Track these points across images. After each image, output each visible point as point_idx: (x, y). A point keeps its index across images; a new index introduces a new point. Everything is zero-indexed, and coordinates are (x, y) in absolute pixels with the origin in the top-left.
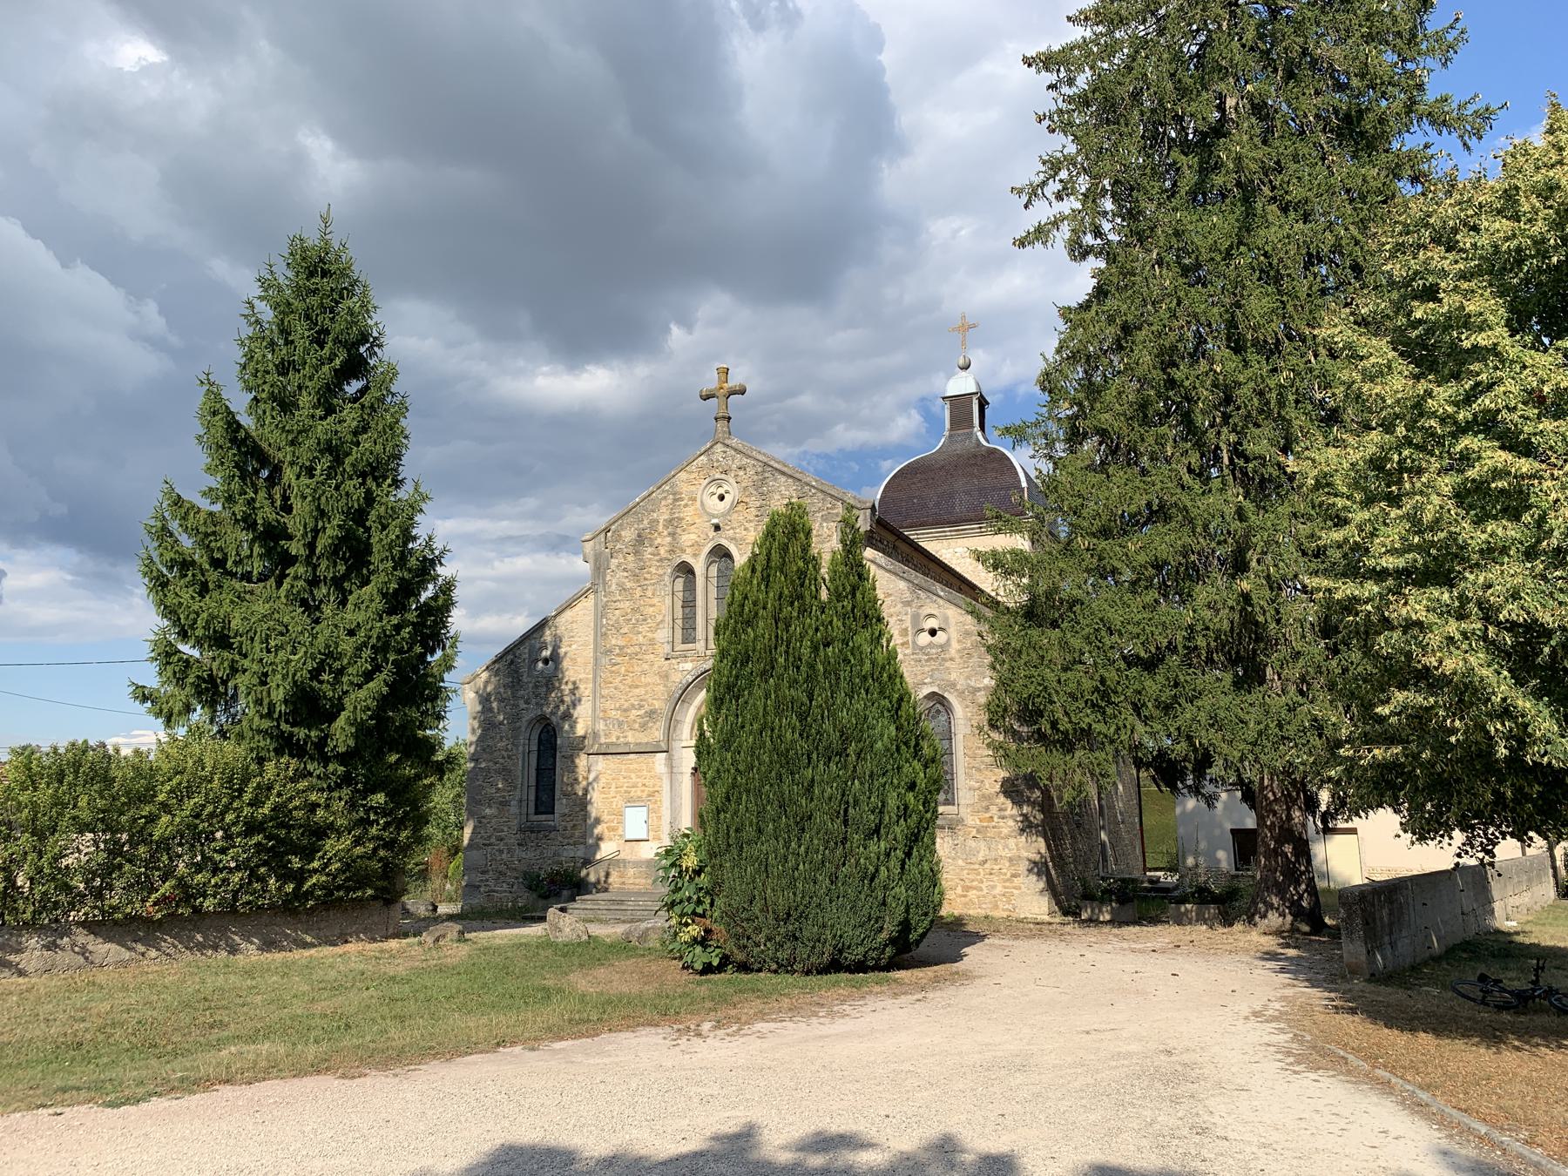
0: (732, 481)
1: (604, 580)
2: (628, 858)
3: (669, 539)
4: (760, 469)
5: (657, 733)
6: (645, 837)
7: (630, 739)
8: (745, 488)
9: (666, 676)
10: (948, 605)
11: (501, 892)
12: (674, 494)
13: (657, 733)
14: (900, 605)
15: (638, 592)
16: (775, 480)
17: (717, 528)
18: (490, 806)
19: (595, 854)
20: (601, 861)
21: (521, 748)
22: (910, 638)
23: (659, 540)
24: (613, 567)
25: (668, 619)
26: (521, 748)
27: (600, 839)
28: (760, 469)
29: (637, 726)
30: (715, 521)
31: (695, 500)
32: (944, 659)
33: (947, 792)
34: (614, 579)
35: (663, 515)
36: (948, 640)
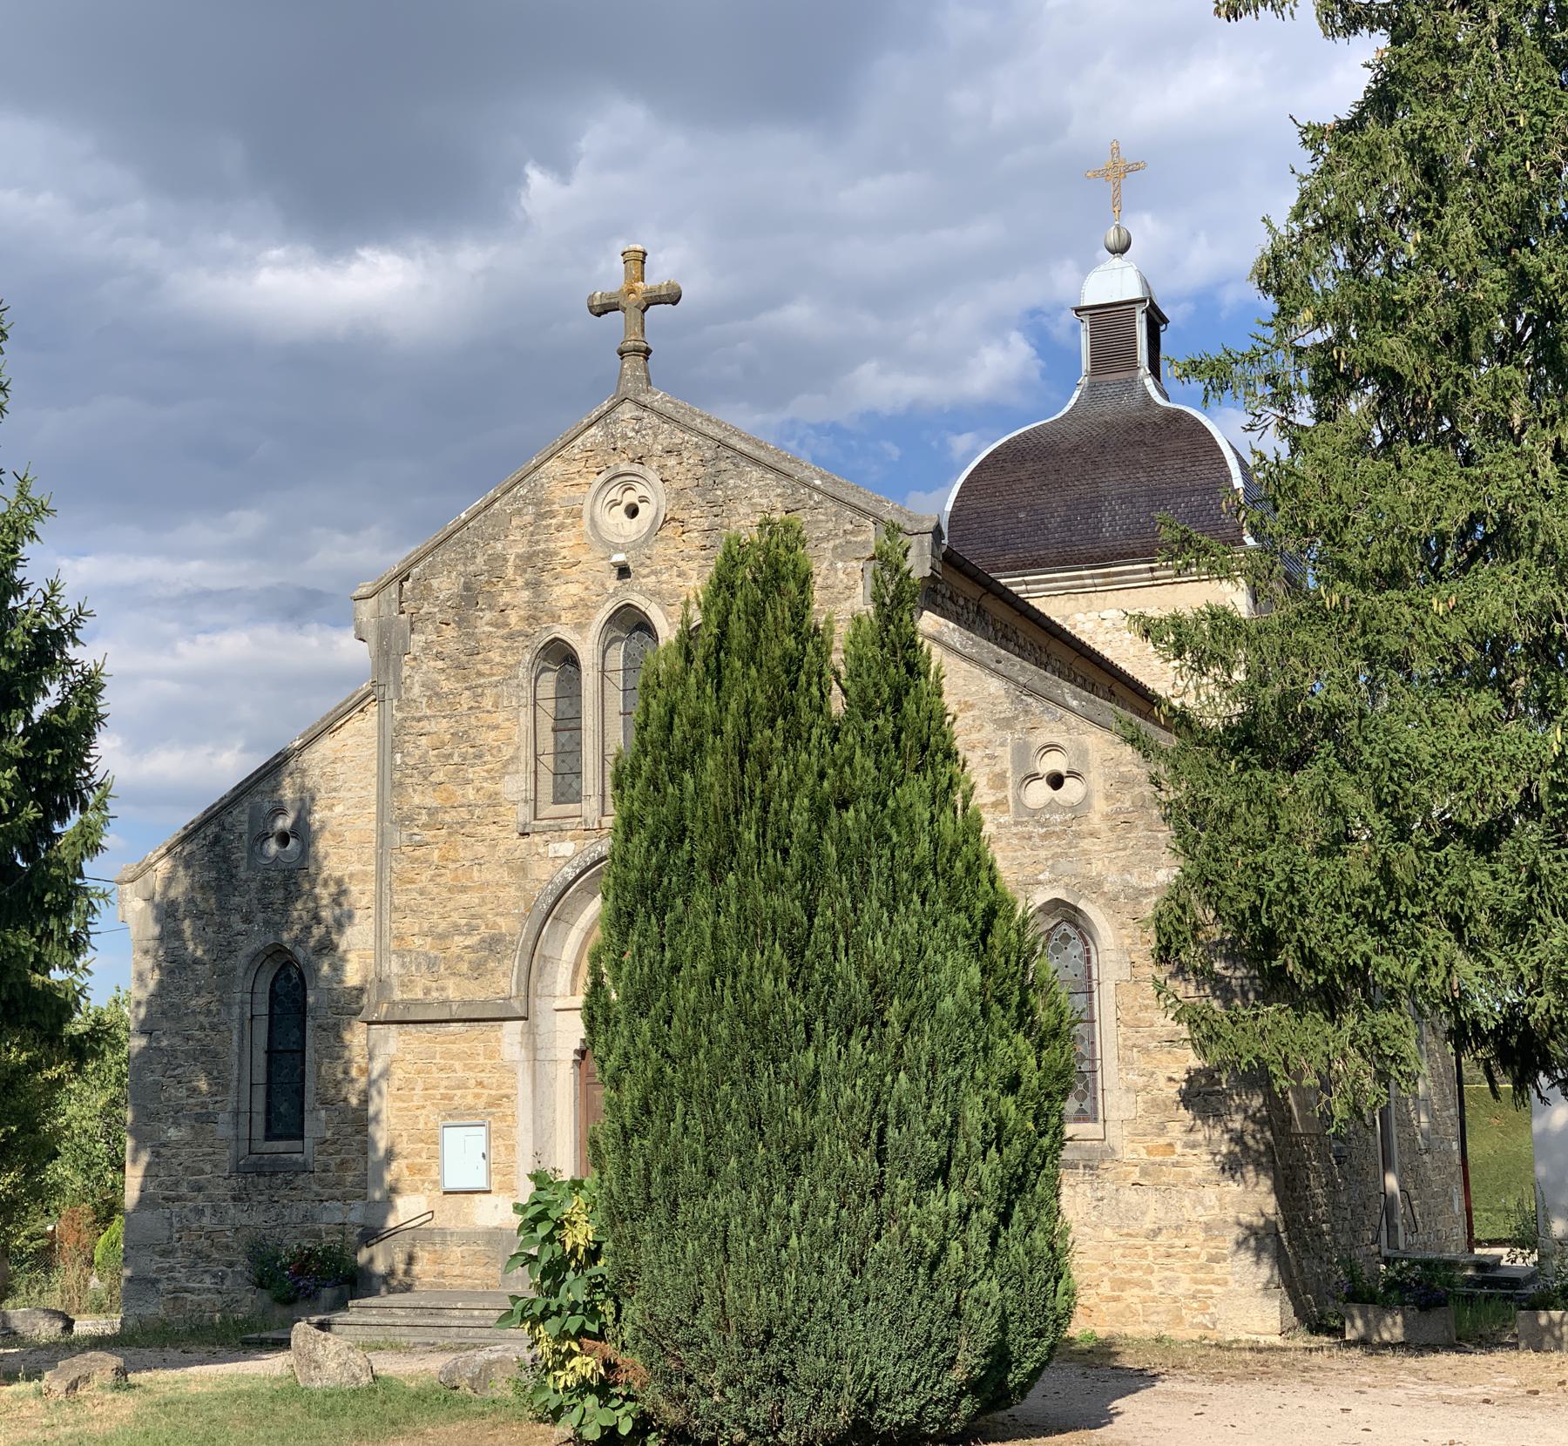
0: (654, 477)
1: (397, 675)
2: (452, 1225)
3: (526, 595)
5: (504, 983)
6: (483, 1185)
7: (452, 993)
9: (520, 869)
10: (1086, 726)
11: (200, 1292)
12: (538, 504)
13: (504, 982)
14: (989, 727)
15: (466, 700)
16: (740, 475)
17: (623, 571)
18: (177, 1124)
19: (385, 1217)
20: (396, 1231)
21: (236, 1010)
22: (1010, 792)
23: (507, 597)
24: (415, 650)
25: (526, 754)
26: (236, 1010)
27: (393, 1190)
28: (708, 454)
29: (464, 967)
30: (619, 558)
31: (579, 515)
32: (1078, 835)
33: (1082, 1097)
34: (419, 673)
35: (514, 547)
36: (1087, 796)
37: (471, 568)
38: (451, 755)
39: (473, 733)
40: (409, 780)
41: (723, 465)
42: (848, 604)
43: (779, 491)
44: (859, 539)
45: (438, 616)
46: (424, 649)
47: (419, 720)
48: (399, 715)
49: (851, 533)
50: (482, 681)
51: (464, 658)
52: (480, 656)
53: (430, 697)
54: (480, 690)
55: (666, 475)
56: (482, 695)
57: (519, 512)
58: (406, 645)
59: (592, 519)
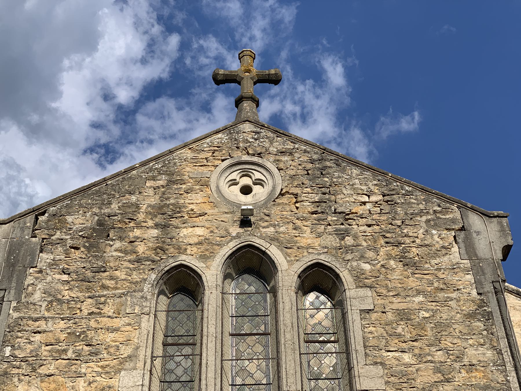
3: (155, 232)
4: (315, 157)
8: (293, 177)
15: (88, 306)
16: (343, 171)
23: (137, 232)
25: (144, 353)
37: (106, 211)
38: (65, 351)
39: (91, 334)
40: (15, 371)
41: (328, 164)
42: (446, 258)
43: (375, 182)
44: (448, 217)
45: (69, 241)
46: (50, 265)
47: (36, 320)
48: (16, 315)
49: (440, 212)
50: (105, 293)
51: (89, 274)
52: (107, 274)
53: (51, 302)
54: (103, 299)
55: (281, 165)
56: (104, 303)
57: (154, 179)
58: (33, 260)
59: (218, 187)
